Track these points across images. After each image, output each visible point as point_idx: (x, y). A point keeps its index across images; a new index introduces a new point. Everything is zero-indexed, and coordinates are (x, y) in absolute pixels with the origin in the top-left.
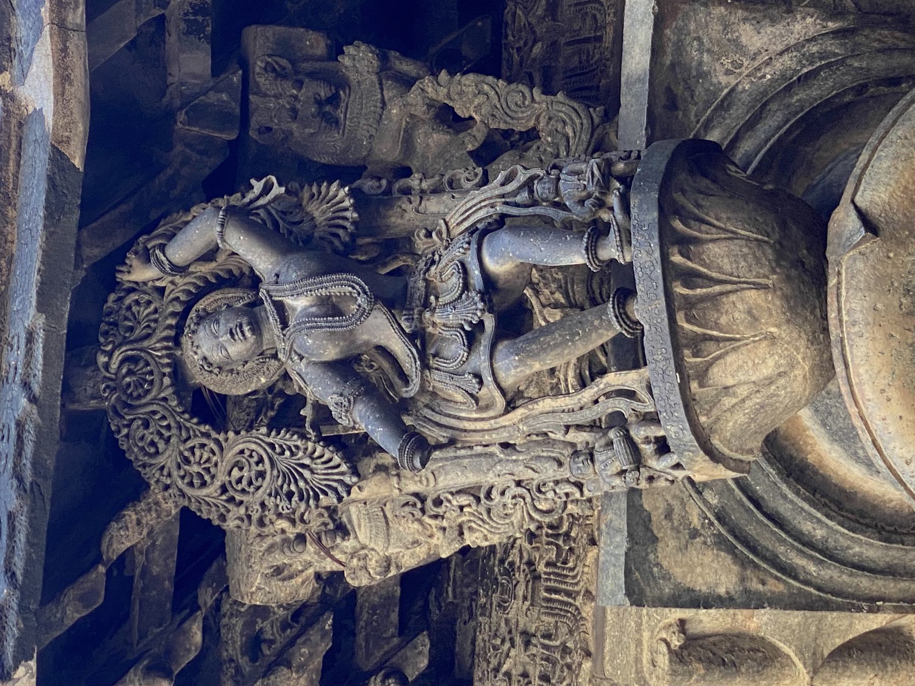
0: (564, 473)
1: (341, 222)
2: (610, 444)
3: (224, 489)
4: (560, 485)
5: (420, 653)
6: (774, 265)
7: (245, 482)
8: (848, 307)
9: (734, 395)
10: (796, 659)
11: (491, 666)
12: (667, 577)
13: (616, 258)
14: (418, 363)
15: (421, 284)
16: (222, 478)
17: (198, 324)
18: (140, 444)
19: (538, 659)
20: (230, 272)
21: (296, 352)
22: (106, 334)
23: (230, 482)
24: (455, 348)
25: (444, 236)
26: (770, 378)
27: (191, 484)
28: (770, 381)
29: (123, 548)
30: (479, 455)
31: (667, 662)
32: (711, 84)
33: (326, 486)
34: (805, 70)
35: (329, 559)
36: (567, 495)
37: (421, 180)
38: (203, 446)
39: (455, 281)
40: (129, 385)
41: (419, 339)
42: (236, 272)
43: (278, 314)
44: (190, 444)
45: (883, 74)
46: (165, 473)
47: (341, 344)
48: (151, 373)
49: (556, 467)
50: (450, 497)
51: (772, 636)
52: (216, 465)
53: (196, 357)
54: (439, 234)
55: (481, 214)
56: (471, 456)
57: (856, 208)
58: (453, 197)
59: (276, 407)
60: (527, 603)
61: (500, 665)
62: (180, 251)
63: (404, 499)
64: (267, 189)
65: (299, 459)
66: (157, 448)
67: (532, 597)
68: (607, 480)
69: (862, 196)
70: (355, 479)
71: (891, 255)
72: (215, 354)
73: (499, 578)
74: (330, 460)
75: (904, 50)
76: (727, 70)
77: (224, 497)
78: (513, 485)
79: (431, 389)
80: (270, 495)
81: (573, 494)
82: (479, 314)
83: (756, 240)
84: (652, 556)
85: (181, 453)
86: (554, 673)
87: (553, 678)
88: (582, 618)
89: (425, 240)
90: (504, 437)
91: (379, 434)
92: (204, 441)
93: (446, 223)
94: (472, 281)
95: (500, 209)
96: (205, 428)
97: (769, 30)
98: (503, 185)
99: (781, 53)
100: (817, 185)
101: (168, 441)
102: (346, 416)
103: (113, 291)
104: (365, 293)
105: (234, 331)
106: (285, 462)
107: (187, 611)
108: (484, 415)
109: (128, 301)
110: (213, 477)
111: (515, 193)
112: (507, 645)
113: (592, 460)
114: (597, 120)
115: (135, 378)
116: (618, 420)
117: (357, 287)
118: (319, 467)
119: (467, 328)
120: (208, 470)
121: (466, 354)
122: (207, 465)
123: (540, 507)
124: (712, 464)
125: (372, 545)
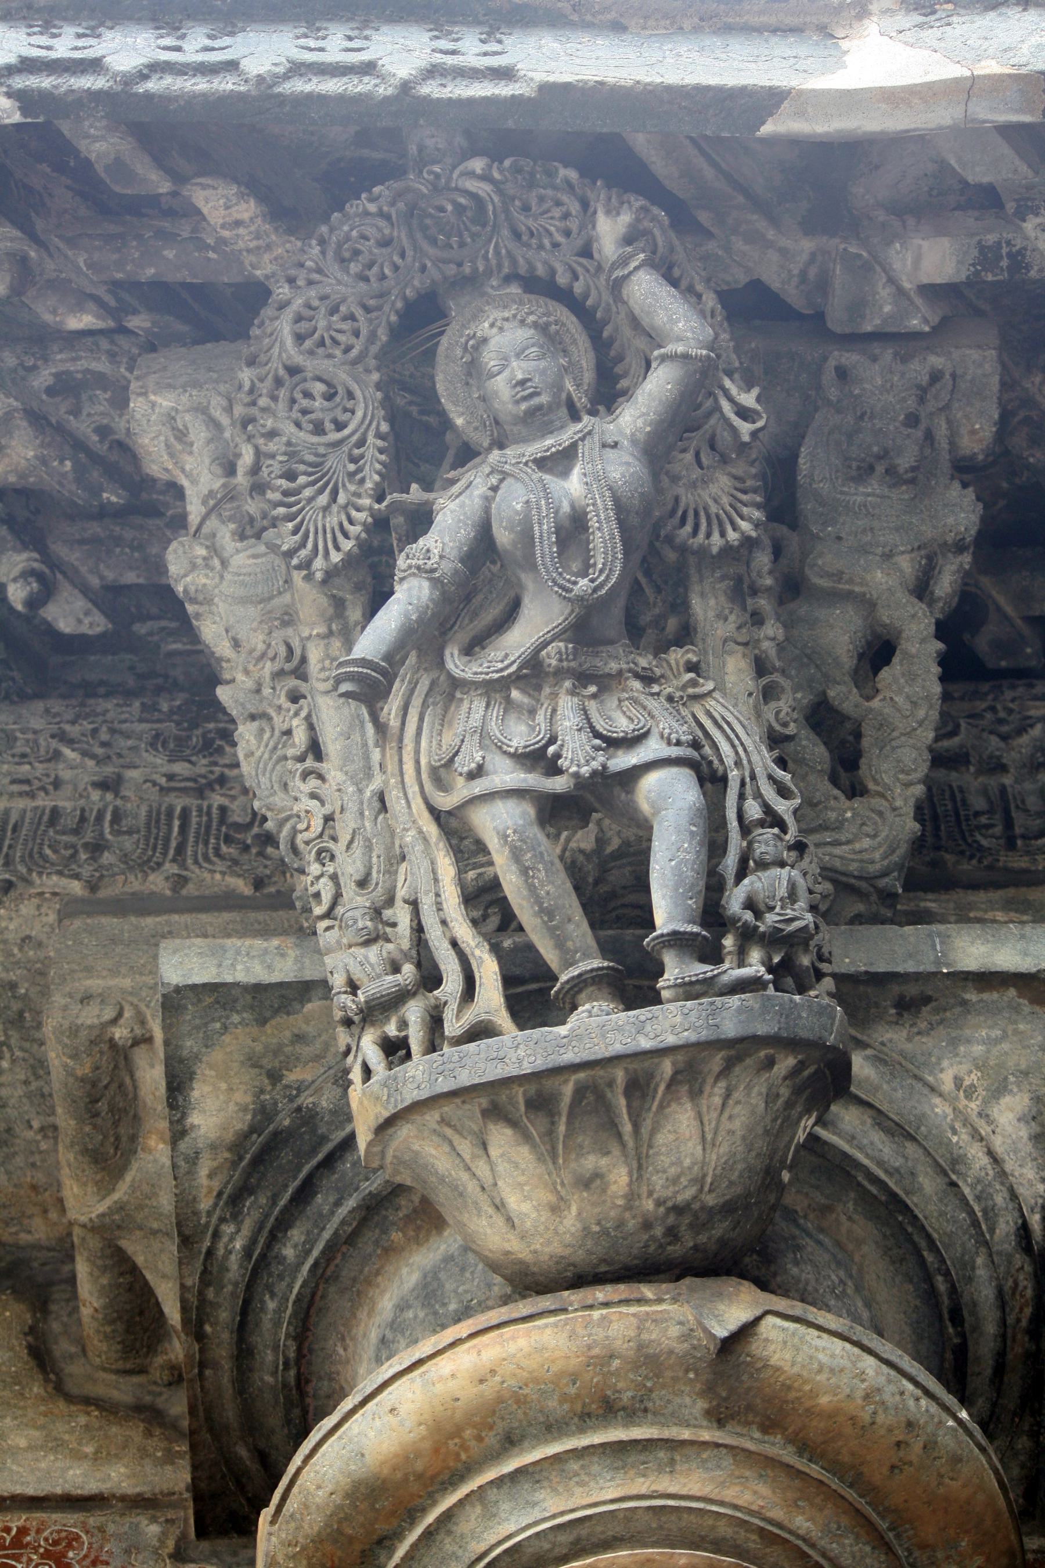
0: (349, 890)
2: (396, 969)
3: (293, 371)
4: (330, 884)
5: (80, 621)
6: (670, 1204)
7: (305, 403)
8: (614, 1318)
9: (474, 1157)
10: (108, 1202)
11: (67, 727)
12: (208, 1043)
14: (496, 676)
15: (613, 666)
16: (311, 365)
17: (535, 325)
18: (354, 233)
19: (82, 802)
20: (620, 359)
21: (501, 481)
22: (517, 170)
23: (305, 380)
24: (520, 735)
26: (503, 1204)
27: (299, 319)
28: (500, 1206)
29: (200, 203)
30: (367, 757)
31: (89, 1022)
32: (939, 1059)
33: (307, 531)
34: (967, 1191)
35: (203, 510)
37: (773, 639)
38: (357, 334)
39: (622, 725)
40: (442, 209)
41: (532, 673)
42: (618, 369)
44: (359, 313)
45: (966, 1298)
46: (316, 277)
48: (462, 245)
49: (357, 877)
50: (303, 714)
51: (140, 1169)
52: (330, 356)
54: (694, 683)
55: (725, 747)
56: (365, 745)
57: (758, 1320)
59: (425, 418)
60: (163, 781)
61: (70, 742)
62: (646, 290)
66: (350, 260)
67: (175, 789)
69: (774, 1326)
70: (319, 576)
71: (691, 1375)
73: (199, 732)
74: (346, 536)
75: (1003, 1322)
76: (962, 1080)
77: (281, 372)
78: (327, 810)
79: (458, 695)
80: (289, 444)
81: (320, 903)
82: (574, 769)
83: (704, 1176)
84: (236, 1018)
85: (344, 300)
86: (64, 833)
87: (57, 832)
88: (146, 875)
89: (682, 662)
90: (394, 797)
91: (390, 620)
92: (364, 332)
93: (710, 692)
94: (620, 753)
95: (734, 774)
96: (383, 336)
97: (1024, 1133)
98: (770, 777)
99: (990, 1153)
100: (798, 1226)
102: (410, 567)
103: (582, 175)
104: (595, 590)
106: (337, 463)
107: (113, 303)
108: (424, 776)
109: (565, 198)
111: (758, 795)
112: (100, 751)
113: (367, 943)
114: (882, 883)
115: (453, 219)
116: (431, 979)
118: (332, 520)
119: (551, 750)
120: (322, 343)
122: (328, 341)
124: (373, 1124)
125: (228, 577)
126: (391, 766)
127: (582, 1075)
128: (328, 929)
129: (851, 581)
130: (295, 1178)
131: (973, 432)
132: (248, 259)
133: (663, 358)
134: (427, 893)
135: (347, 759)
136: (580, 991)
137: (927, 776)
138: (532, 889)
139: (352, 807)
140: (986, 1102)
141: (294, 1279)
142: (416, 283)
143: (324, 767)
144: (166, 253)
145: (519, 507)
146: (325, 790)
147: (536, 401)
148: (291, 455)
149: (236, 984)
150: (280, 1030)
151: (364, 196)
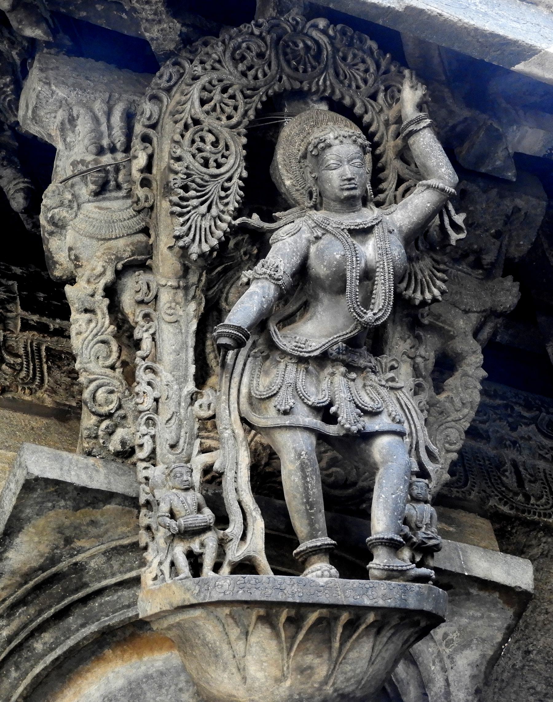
1: (413, 286)
3: (196, 122)
4: (151, 440)
6: (341, 692)
7: (201, 145)
9: (239, 638)
13: (375, 561)
14: (307, 355)
16: (208, 121)
18: (244, 45)
21: (323, 234)
23: (202, 130)
25: (390, 384)
26: (244, 669)
27: (204, 88)
28: (241, 669)
30: (186, 369)
36: (141, 446)
38: (236, 108)
42: (381, 175)
43: (364, 228)
44: (239, 96)
46: (217, 65)
47: (327, 282)
48: (305, 71)
50: (151, 331)
52: (219, 119)
53: (331, 136)
54: (393, 379)
56: (187, 361)
58: (411, 390)
63: (153, 286)
64: (456, 228)
65: (216, 204)
68: (168, 499)
72: (333, 156)
77: (190, 121)
78: (156, 394)
84: (62, 503)
85: (231, 85)
89: (389, 365)
92: (241, 110)
93: (400, 388)
96: (251, 114)
97: (468, 673)
98: (427, 449)
99: (447, 680)
101: (244, 74)
102: (265, 273)
103: (379, 48)
105: (353, 181)
106: (214, 188)
107: (52, 26)
109: (369, 60)
110: (208, 113)
115: (302, 53)
116: (222, 520)
117: (380, 314)
118: (206, 224)
120: (214, 109)
121: (310, 403)
123: (100, 391)
125: (81, 216)
126: (224, 388)
127: (324, 611)
128: (145, 468)
129: (444, 322)
130: (58, 603)
131: (518, 245)
132: (144, 25)
133: (429, 187)
134: (231, 470)
135: (176, 367)
136: (314, 555)
137: (461, 449)
138: (306, 489)
139: (175, 398)
140: (456, 651)
141: (37, 663)
142: (276, 87)
143: (158, 366)
144: (97, 6)
145: (338, 257)
146: (157, 381)
147: (352, 192)
148: (188, 175)
149: (71, 484)
150: (86, 515)
151: (253, 22)
